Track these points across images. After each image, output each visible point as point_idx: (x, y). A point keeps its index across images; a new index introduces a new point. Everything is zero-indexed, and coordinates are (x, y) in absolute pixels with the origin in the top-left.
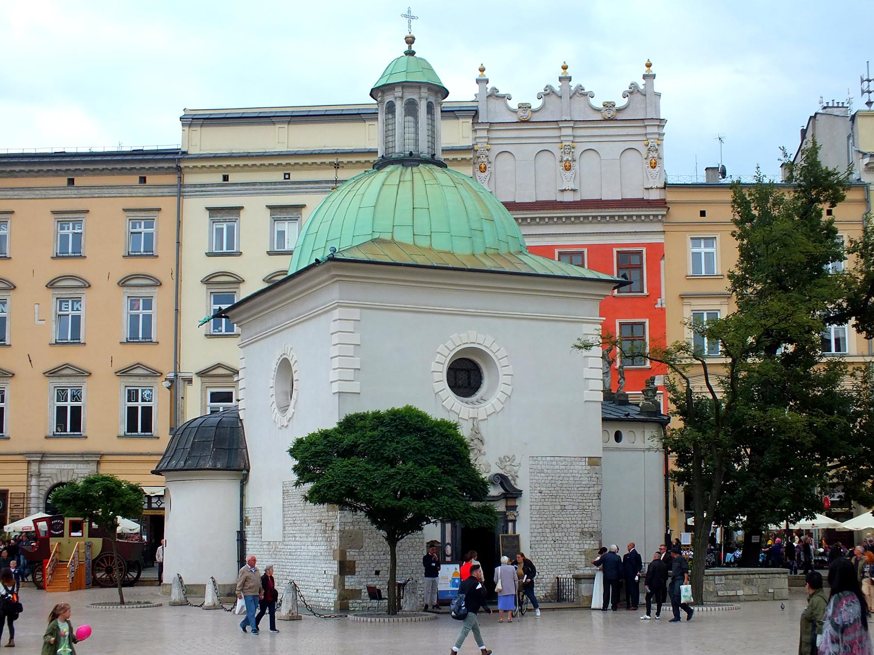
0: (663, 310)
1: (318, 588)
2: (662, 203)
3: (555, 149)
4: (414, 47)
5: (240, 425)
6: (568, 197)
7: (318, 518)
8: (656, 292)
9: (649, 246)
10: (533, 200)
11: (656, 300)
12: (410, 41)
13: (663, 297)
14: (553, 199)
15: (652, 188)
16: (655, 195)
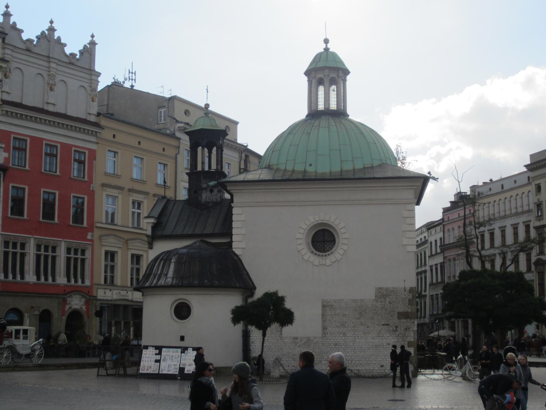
0: (93, 191)
1: (384, 364)
2: (96, 125)
3: (45, 74)
4: (329, 46)
5: (236, 258)
6: (51, 108)
7: (383, 323)
8: (91, 181)
9: (90, 150)
10: (32, 105)
11: (90, 185)
12: (326, 41)
13: (94, 184)
14: (41, 107)
15: (92, 114)
16: (93, 119)
